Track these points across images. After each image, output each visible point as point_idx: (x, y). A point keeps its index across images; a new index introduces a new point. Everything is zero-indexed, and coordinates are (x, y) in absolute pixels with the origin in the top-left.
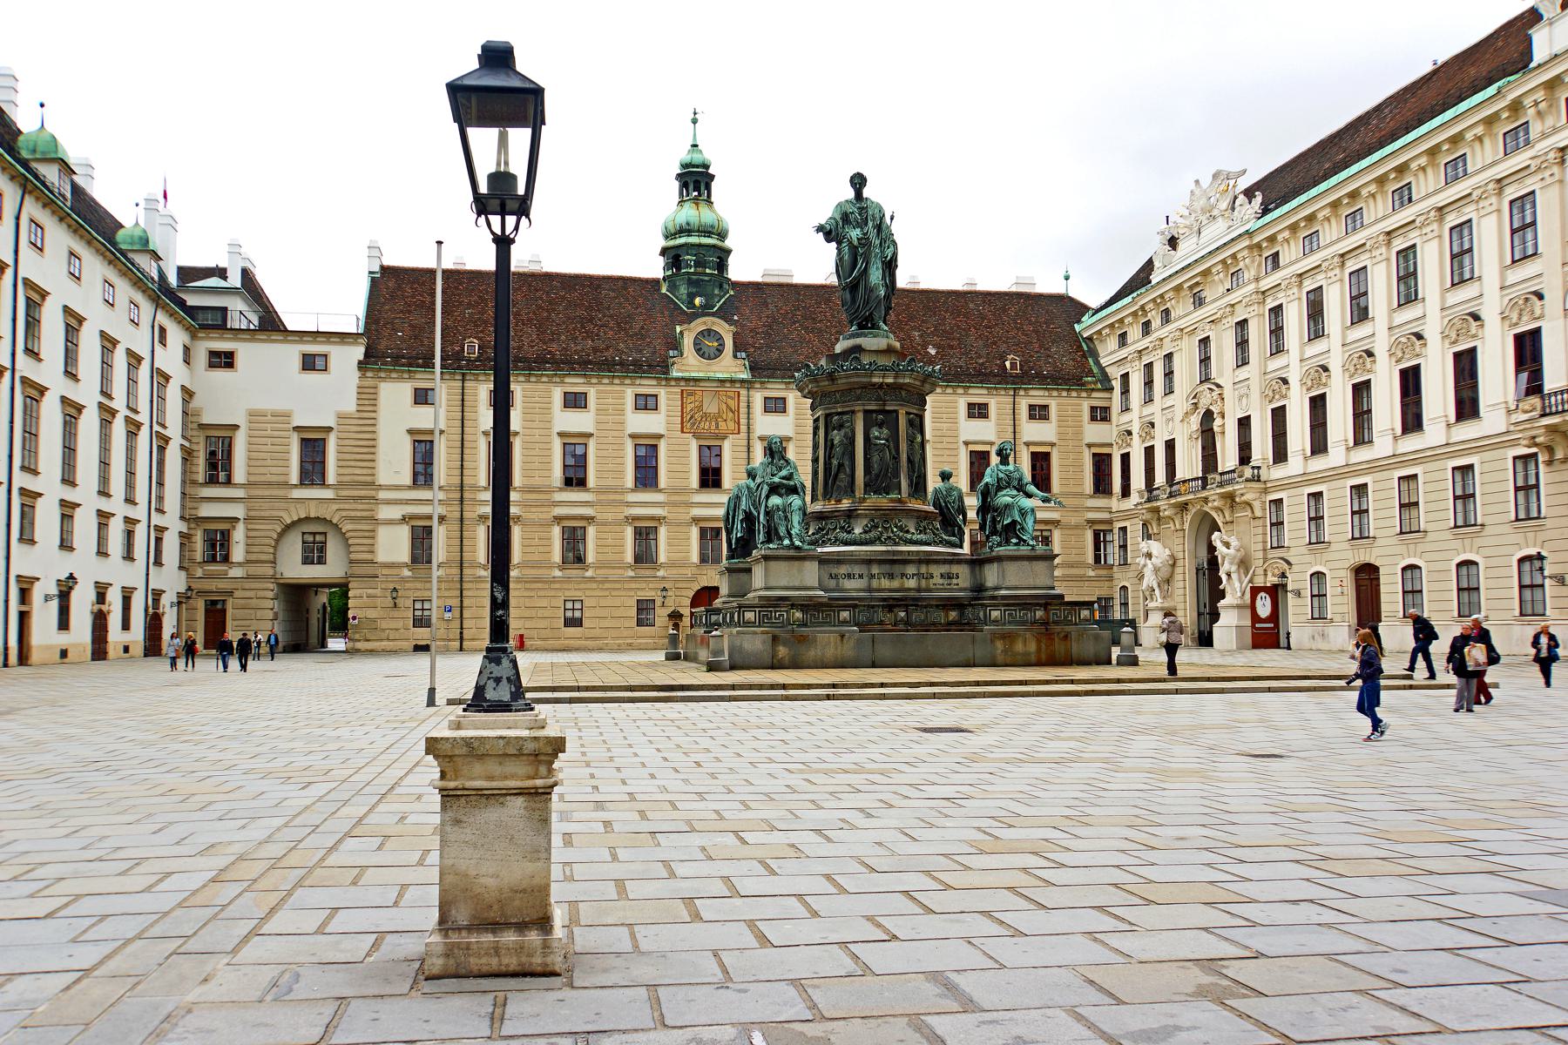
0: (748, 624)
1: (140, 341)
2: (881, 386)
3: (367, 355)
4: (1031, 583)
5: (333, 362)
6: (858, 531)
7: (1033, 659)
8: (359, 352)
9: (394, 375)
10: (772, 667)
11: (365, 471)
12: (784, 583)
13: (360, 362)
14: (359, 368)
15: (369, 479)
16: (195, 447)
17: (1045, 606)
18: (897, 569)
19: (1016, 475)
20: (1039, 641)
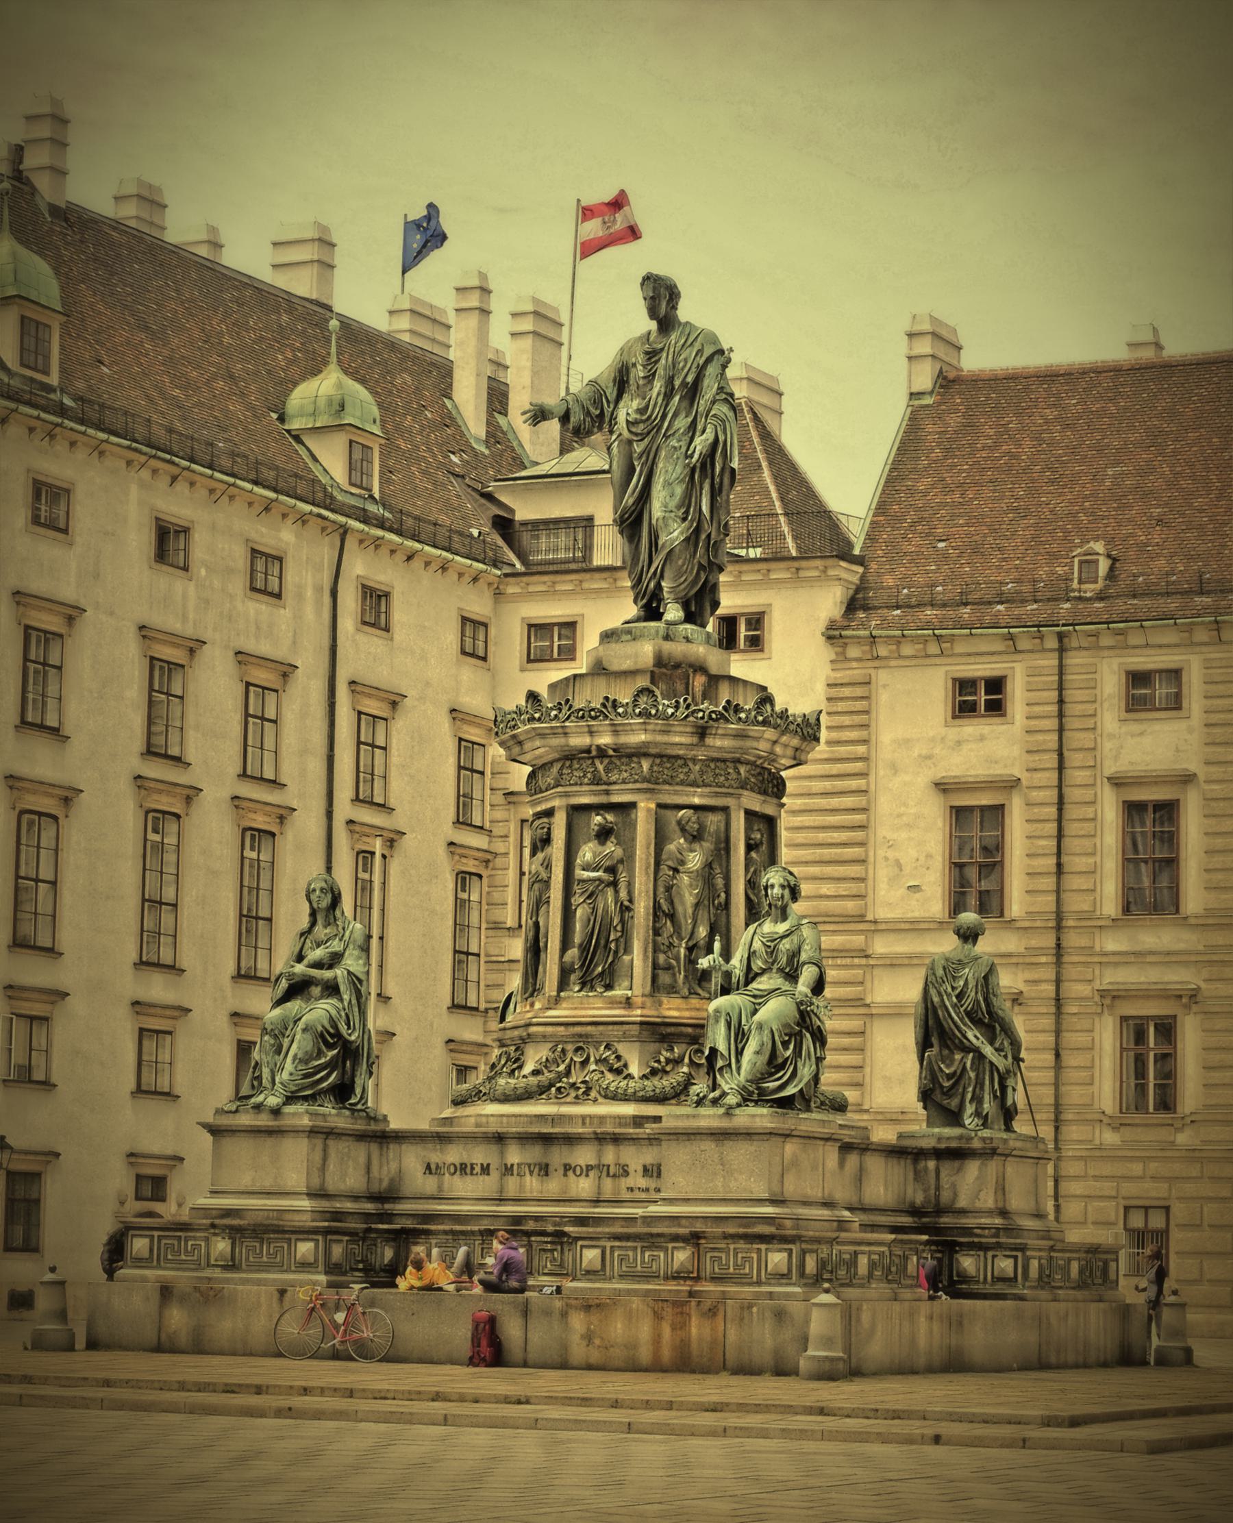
0: (139, 1262)
1: (293, 629)
2: (602, 753)
3: (853, 605)
4: (718, 1187)
5: (776, 632)
6: (528, 1069)
7: (645, 1354)
8: (827, 602)
9: (907, 650)
10: (159, 1349)
11: (843, 889)
12: (246, 1180)
13: (832, 625)
14: (829, 638)
15: (850, 906)
16: (499, 847)
17: (694, 1239)
18: (558, 1156)
19: (785, 945)
20: (658, 1316)
